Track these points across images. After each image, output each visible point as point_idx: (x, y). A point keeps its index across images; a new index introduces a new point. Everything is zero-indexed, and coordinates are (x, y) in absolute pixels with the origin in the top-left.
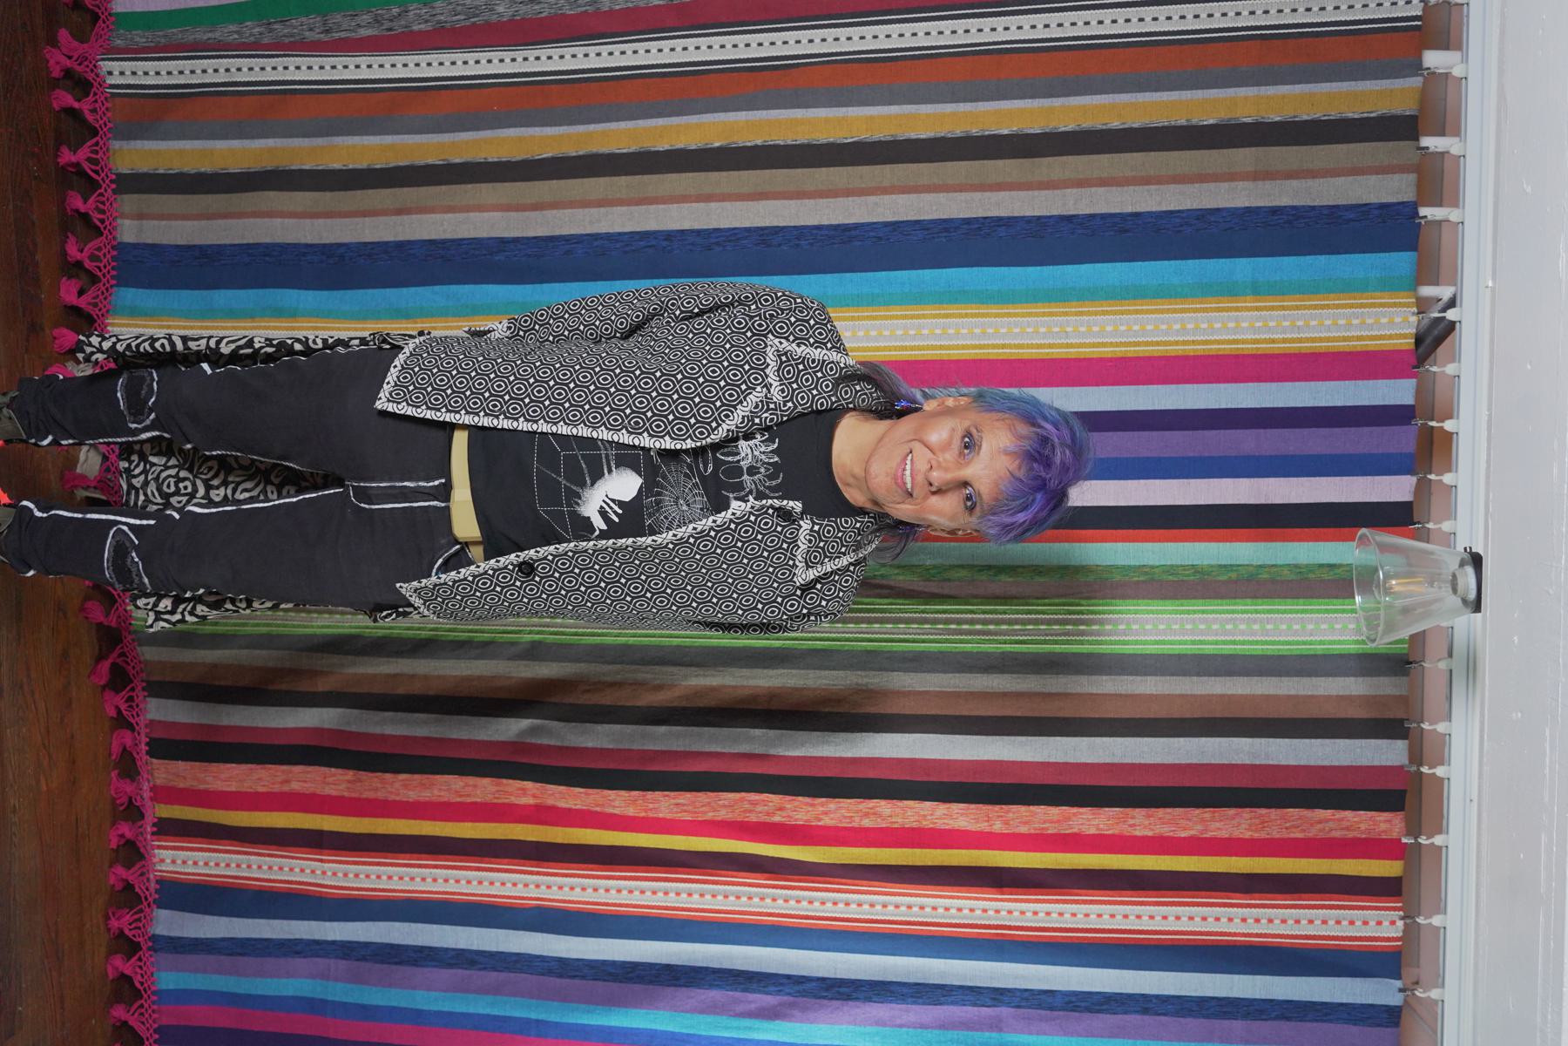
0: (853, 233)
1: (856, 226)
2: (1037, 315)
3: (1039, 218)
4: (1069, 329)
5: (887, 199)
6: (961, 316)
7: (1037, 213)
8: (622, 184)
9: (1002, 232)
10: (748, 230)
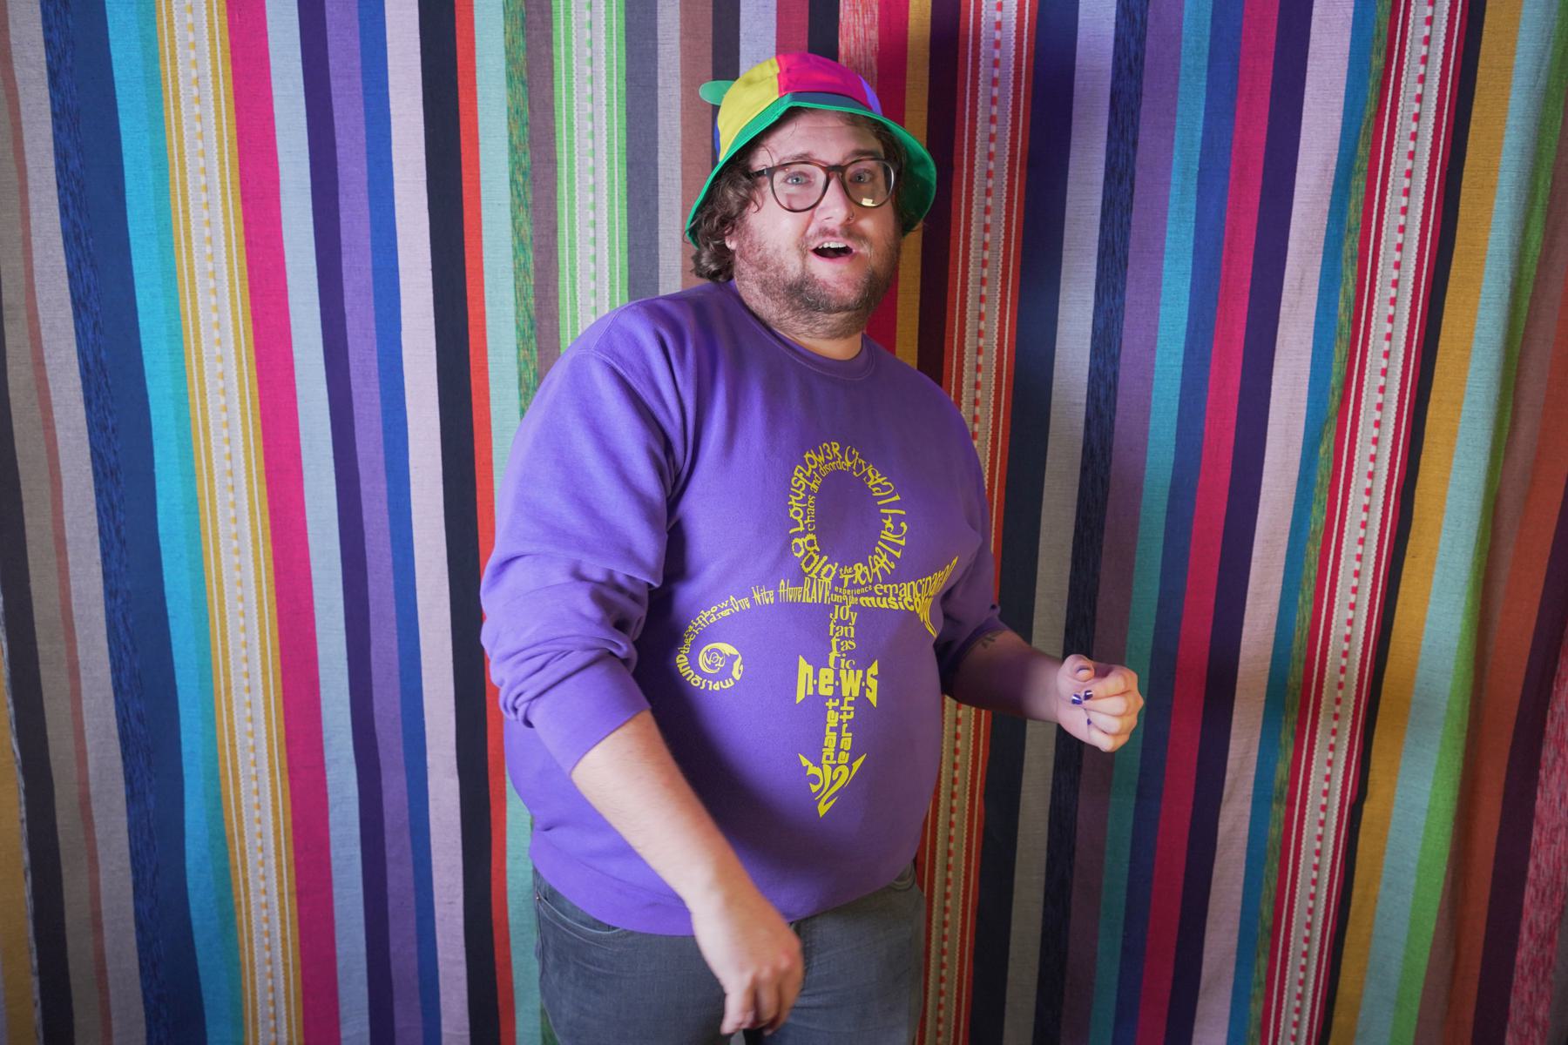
0: (90, 359)
1: (82, 354)
2: (178, 117)
3: (54, 115)
4: (194, 74)
5: (42, 315)
6: (187, 220)
7: (49, 118)
8: (47, 647)
9: (74, 164)
10: (99, 493)
